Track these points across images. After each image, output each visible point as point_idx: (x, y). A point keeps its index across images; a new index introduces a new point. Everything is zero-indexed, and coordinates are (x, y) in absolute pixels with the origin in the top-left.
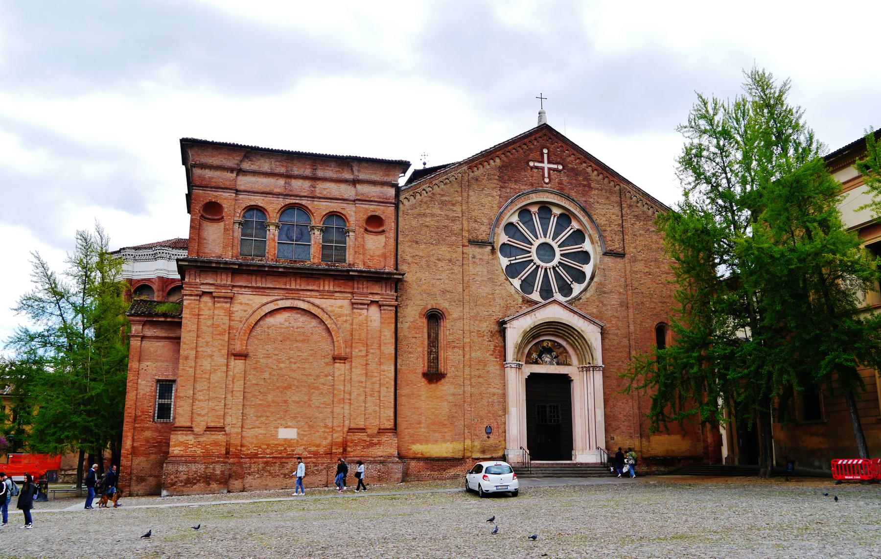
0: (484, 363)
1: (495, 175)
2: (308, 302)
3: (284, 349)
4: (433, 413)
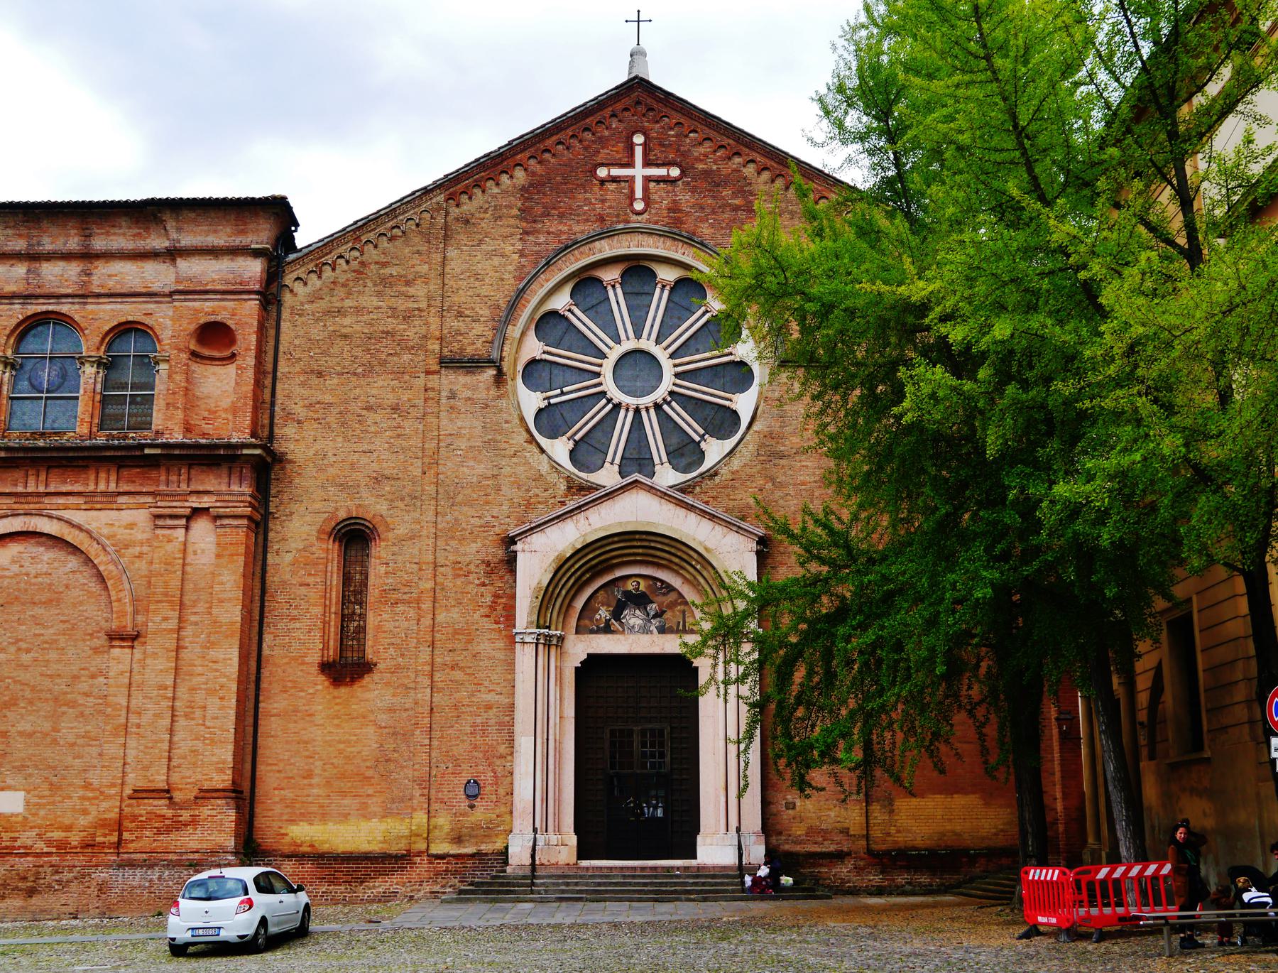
0: (466, 634)
1: (510, 207)
2: (59, 519)
3: (6, 621)
4: (341, 752)
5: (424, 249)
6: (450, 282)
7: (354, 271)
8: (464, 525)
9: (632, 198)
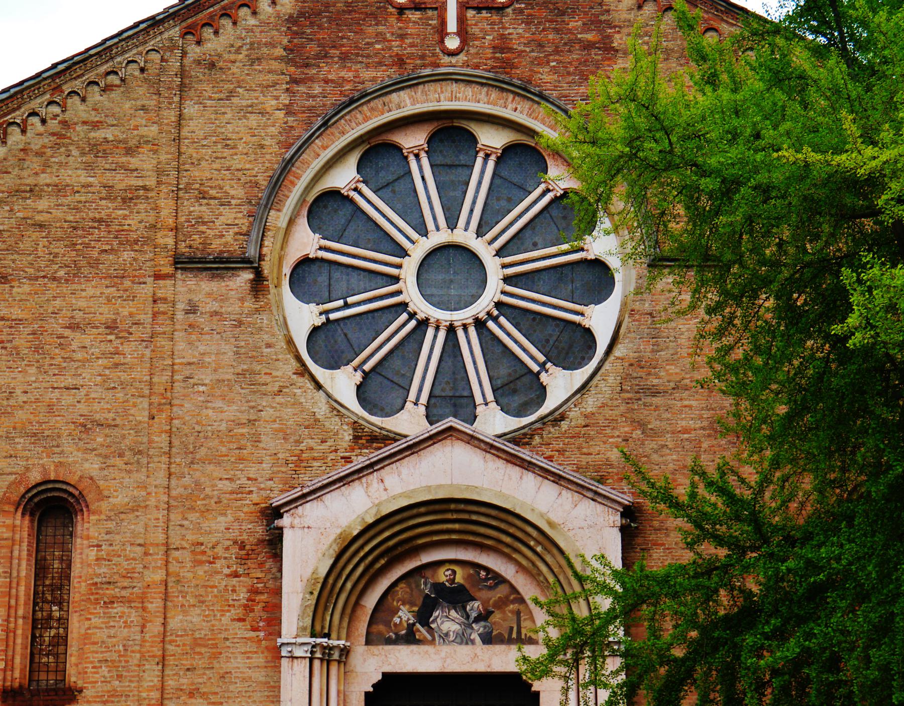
1: (272, 45)
5: (152, 103)
6: (189, 150)
7: (53, 134)
8: (208, 491)
9: (442, 32)
